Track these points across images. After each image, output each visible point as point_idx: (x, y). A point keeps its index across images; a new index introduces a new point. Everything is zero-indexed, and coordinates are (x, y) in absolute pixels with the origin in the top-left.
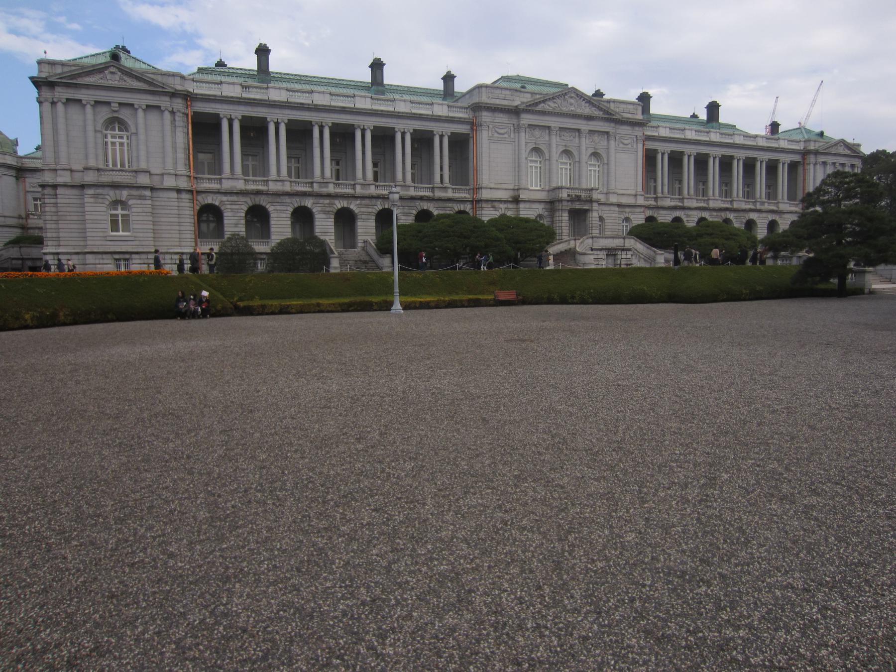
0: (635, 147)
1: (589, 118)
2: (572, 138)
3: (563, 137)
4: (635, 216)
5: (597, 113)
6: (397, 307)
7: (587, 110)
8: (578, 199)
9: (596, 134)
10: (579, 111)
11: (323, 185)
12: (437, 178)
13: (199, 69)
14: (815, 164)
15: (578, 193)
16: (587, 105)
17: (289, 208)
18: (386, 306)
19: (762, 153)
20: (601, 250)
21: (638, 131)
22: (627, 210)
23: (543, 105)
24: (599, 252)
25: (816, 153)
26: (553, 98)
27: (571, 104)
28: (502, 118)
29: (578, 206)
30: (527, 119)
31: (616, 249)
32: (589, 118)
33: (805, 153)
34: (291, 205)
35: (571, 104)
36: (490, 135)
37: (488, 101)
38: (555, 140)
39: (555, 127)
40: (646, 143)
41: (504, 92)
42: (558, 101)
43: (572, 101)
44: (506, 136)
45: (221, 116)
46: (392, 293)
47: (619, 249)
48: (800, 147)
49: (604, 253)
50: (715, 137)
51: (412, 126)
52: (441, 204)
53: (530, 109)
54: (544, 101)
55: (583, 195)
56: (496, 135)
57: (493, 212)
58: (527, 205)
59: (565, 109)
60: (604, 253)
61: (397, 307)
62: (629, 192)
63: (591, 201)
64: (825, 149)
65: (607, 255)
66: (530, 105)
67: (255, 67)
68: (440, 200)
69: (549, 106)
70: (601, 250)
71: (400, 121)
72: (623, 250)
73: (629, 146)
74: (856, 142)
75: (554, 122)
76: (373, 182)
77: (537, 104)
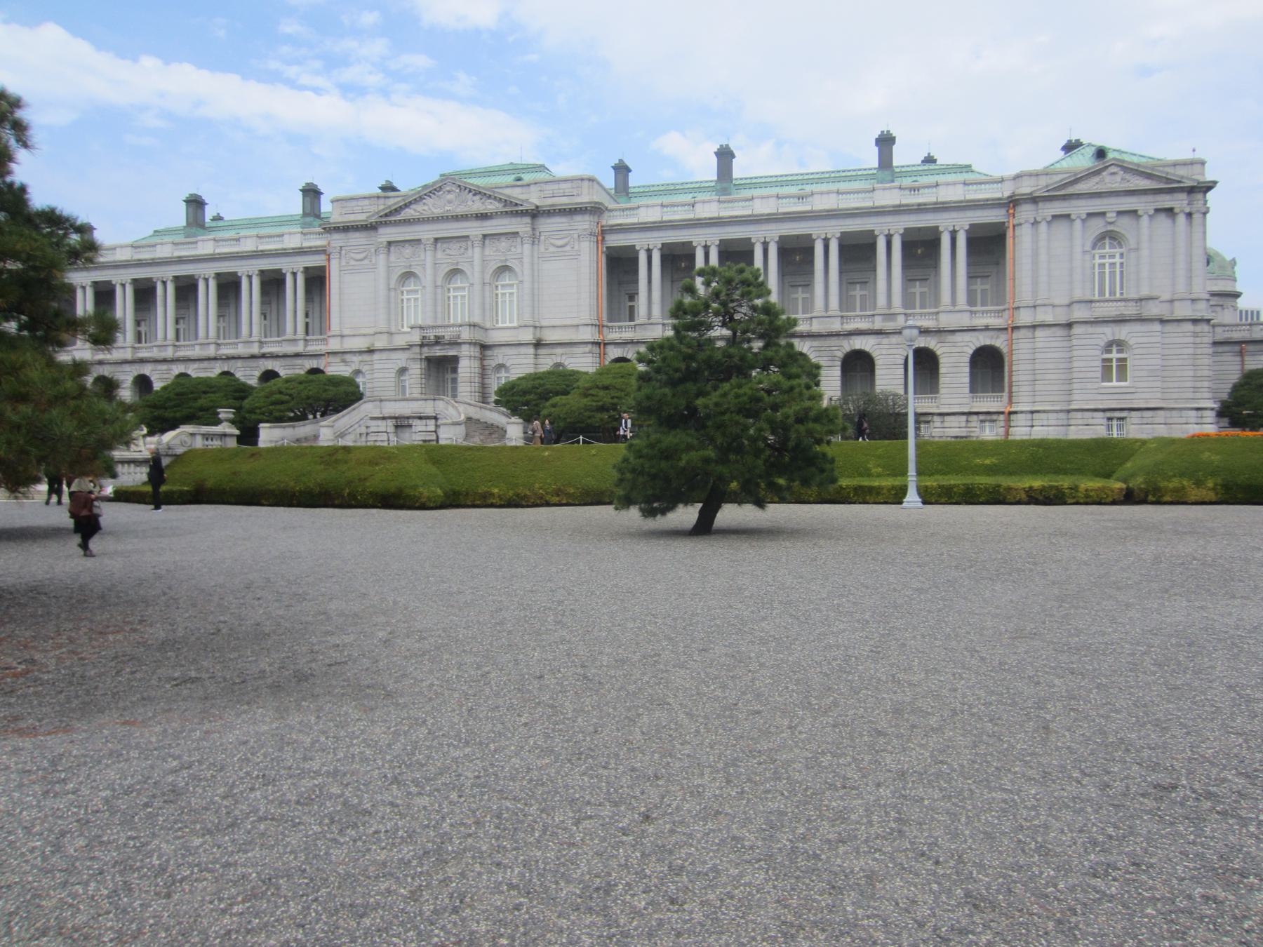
0: (576, 248)
1: (483, 217)
2: (462, 250)
3: (448, 251)
4: (572, 360)
5: (492, 206)
6: (912, 497)
7: (477, 206)
8: (438, 341)
9: (503, 239)
10: (461, 210)
11: (162, 349)
12: (881, 300)
13: (155, 232)
14: (1035, 223)
15: (440, 332)
16: (478, 197)
17: (966, 349)
18: (897, 496)
19: (889, 219)
20: (384, 418)
21: (584, 223)
22: (559, 350)
23: (407, 210)
24: (379, 422)
25: (1034, 200)
26: (421, 198)
27: (450, 202)
28: (358, 238)
29: (438, 352)
30: (387, 234)
31: (408, 418)
32: (483, 217)
33: (1013, 202)
34: (970, 344)
35: (450, 202)
36: (343, 263)
37: (340, 219)
38: (429, 257)
39: (428, 239)
40: (608, 237)
41: (360, 203)
42: (428, 201)
43: (450, 197)
44: (366, 262)
45: (753, 241)
46: (904, 473)
47: (414, 418)
48: (1006, 191)
49: (390, 423)
50: (205, 247)
51: (898, 225)
52: (289, 361)
53: (389, 218)
54: (407, 206)
55: (447, 334)
56: (352, 262)
57: (343, 368)
58: (384, 355)
59: (437, 212)
60: (390, 423)
61: (912, 497)
62: (568, 322)
63: (455, 344)
64: (1055, 189)
65: (397, 427)
66: (386, 215)
67: (874, 163)
68: (285, 356)
69: (415, 210)
70: (384, 418)
71: (244, 262)
72: (420, 418)
73: (568, 248)
74: (1198, 155)
75: (427, 233)
76: (968, 308)
77: (397, 211)
